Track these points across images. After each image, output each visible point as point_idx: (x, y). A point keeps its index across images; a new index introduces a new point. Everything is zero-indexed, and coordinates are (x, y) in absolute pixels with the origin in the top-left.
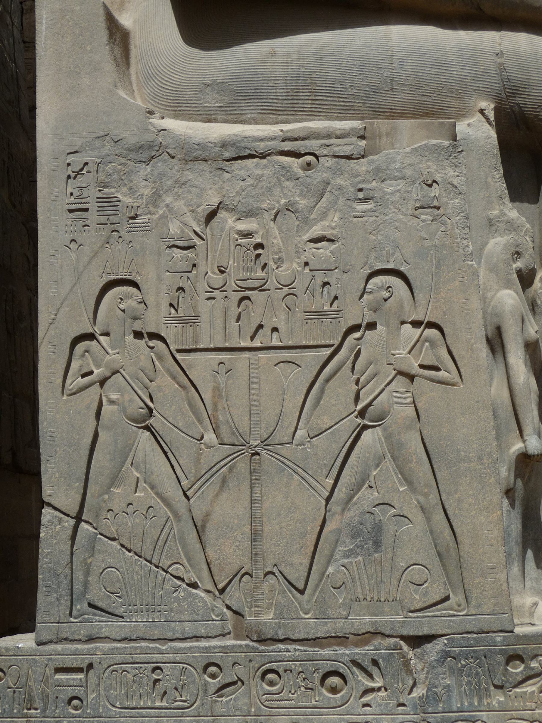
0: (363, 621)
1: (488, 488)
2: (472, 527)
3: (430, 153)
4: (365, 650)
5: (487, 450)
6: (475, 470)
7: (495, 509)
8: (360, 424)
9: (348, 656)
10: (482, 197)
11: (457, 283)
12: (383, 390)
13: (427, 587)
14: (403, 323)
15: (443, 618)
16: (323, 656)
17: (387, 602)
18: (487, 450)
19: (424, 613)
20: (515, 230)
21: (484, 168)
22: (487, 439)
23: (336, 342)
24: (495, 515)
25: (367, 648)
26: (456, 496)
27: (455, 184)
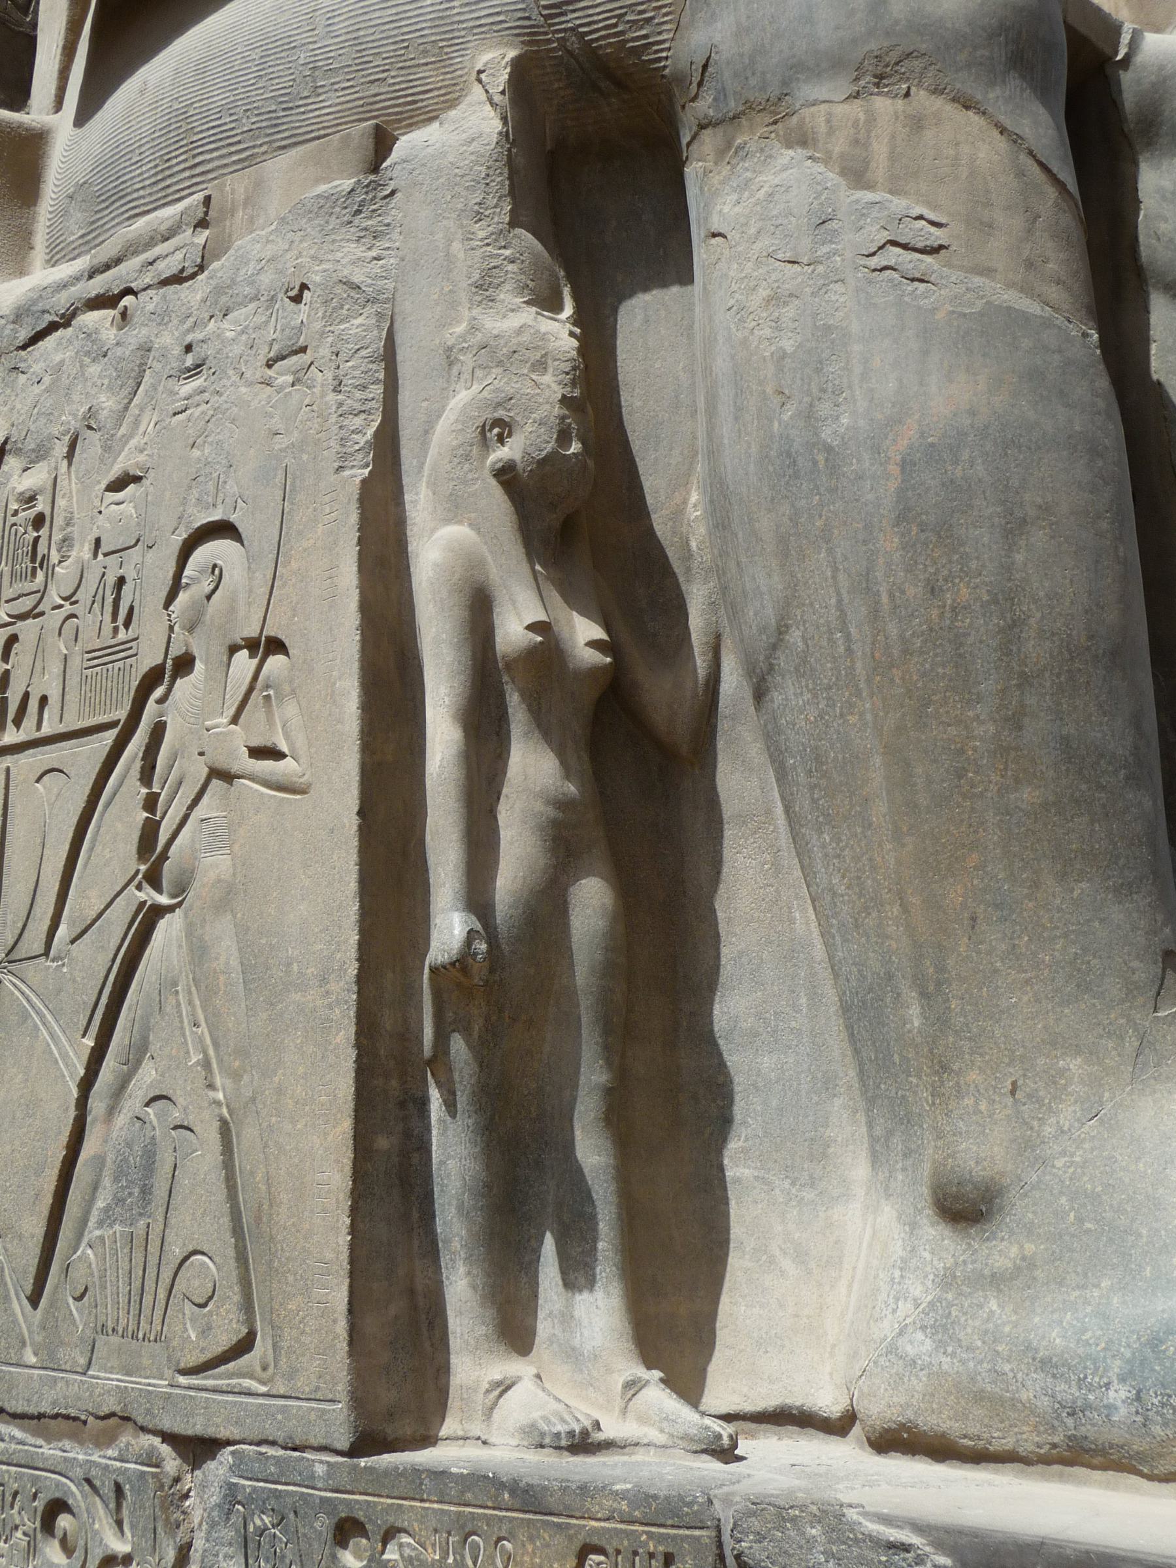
0: (107, 1384)
1: (331, 1059)
2: (296, 1160)
3: (310, 220)
4: (104, 1457)
5: (339, 956)
6: (314, 1010)
7: (339, 1116)
8: (145, 902)
9: (81, 1466)
10: (436, 297)
11: (320, 529)
12: (185, 818)
13: (210, 1313)
14: (233, 649)
15: (230, 1398)
16: (47, 1459)
17: (147, 1342)
18: (339, 956)
19: (205, 1378)
20: (500, 363)
21: (445, 222)
22: (340, 927)
23: (122, 714)
24: (339, 1129)
25: (110, 1453)
26: (276, 1079)
27: (356, 279)
